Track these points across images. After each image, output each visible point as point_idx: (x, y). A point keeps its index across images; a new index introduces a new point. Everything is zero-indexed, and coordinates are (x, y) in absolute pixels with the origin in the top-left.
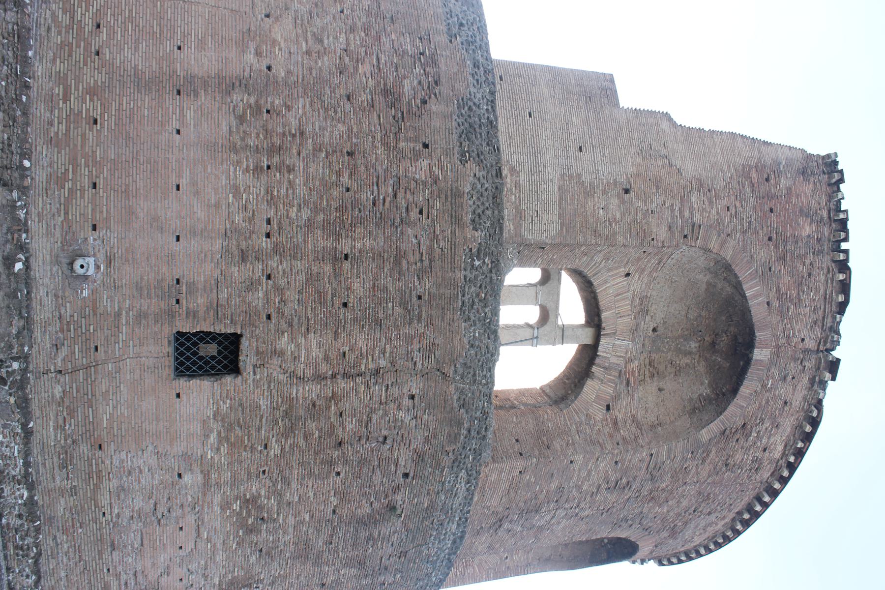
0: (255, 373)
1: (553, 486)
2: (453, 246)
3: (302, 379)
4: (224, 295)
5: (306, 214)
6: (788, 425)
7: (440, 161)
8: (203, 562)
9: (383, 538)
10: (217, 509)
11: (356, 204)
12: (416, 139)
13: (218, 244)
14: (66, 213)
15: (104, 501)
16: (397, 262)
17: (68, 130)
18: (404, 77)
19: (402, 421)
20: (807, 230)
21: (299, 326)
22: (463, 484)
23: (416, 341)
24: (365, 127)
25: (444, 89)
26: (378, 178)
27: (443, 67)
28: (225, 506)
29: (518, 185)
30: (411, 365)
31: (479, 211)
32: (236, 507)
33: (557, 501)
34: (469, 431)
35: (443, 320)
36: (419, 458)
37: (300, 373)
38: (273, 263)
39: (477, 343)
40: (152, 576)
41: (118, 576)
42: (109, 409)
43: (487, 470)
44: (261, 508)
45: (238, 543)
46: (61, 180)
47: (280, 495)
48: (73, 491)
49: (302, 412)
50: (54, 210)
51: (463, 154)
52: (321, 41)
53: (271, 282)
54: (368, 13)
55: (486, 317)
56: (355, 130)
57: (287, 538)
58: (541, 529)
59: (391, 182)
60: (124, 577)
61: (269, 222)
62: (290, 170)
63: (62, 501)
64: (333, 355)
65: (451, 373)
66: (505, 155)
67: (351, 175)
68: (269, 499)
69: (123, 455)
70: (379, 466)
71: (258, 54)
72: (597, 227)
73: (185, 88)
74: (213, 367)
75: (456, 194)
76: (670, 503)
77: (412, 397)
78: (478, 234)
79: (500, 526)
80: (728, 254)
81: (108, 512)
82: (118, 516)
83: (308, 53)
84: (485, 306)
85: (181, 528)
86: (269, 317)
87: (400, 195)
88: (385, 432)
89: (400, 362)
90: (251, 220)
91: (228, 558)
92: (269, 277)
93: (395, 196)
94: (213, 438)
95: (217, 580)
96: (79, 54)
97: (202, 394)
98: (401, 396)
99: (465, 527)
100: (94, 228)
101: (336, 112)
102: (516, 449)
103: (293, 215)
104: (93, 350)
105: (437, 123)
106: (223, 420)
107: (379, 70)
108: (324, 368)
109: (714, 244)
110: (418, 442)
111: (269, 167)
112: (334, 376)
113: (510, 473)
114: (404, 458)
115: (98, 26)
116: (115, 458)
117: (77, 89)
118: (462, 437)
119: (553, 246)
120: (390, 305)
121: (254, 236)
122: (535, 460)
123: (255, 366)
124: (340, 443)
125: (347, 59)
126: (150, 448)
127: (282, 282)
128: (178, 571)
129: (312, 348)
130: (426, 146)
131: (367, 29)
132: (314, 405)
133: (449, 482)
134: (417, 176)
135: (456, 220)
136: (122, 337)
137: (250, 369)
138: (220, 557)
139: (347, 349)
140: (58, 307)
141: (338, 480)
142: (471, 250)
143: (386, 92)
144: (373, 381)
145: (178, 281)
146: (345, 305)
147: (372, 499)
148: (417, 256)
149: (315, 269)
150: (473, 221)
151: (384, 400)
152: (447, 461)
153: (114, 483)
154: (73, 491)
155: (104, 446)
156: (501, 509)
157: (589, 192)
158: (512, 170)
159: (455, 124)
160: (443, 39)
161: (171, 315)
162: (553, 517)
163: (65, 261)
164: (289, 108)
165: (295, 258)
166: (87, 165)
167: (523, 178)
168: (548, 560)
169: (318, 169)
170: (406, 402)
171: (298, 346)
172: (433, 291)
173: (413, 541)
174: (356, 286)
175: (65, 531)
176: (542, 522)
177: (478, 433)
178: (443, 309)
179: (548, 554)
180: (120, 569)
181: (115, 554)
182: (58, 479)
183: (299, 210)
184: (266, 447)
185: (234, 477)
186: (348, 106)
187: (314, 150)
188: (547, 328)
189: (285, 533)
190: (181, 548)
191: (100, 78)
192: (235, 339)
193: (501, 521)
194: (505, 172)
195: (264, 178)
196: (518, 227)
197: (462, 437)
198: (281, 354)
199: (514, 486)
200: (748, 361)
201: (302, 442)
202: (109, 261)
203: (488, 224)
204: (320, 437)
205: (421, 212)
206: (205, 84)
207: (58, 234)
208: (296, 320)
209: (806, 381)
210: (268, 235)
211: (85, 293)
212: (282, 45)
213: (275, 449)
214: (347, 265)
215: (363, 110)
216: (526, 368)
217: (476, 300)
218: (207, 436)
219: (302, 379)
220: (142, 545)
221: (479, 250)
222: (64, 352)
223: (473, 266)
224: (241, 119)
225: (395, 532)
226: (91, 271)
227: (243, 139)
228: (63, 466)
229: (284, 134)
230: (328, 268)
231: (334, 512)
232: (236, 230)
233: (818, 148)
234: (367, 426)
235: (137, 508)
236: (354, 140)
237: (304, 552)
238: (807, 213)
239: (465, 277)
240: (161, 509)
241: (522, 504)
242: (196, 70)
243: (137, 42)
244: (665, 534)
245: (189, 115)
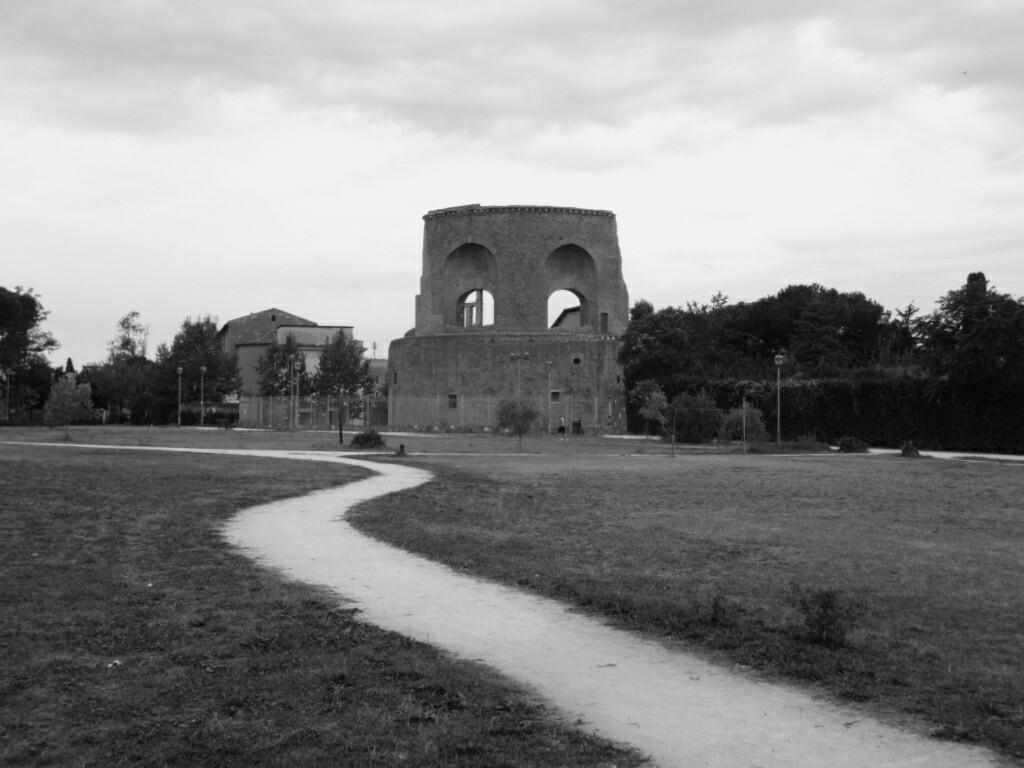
1: (508, 302)
6: (494, 217)
20: (439, 228)
76: (525, 251)
80: (445, 258)
97: (461, 402)
109: (443, 264)
129: (452, 380)
176: (526, 301)
200: (472, 244)
209: (478, 218)
233: (423, 223)
237: (503, 378)
238: (436, 227)
244: (549, 242)
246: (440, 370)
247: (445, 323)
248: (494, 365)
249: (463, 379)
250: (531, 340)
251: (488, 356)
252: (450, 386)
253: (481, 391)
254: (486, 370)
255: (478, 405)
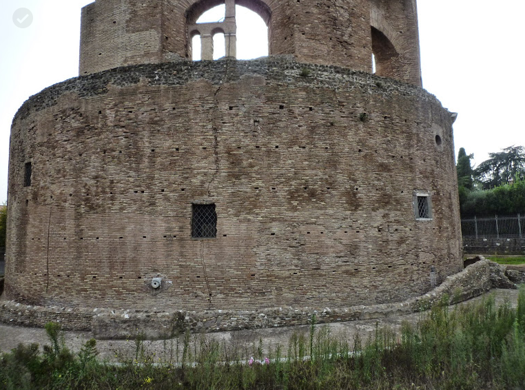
0: (213, 196)
1: (315, 11)
2: (147, 92)
3: (218, 170)
4: (171, 214)
5: (132, 173)
7: (106, 104)
8: (333, 220)
9: (327, 117)
10: (296, 214)
11: (127, 147)
12: (97, 118)
13: (147, 217)
14: (133, 291)
15: (287, 274)
16: (156, 123)
17: (98, 290)
18: (71, 127)
19: (245, 112)
21: (188, 173)
22: (293, 71)
23: (197, 109)
24: (92, 145)
25: (76, 104)
26: (115, 137)
27: (67, 106)
28: (294, 209)
29: (132, 57)
30: (211, 111)
31: (131, 79)
32: (295, 203)
33: (329, 7)
34: (255, 71)
35: (185, 94)
36: (269, 100)
37: (213, 171)
38: (156, 189)
39: (201, 73)
40: (341, 247)
41: (339, 266)
42: (232, 271)
43: (299, 56)
44: (297, 191)
45: (322, 201)
46: (119, 293)
47: (289, 179)
48: (279, 289)
49: (237, 170)
50: (131, 296)
51: (104, 92)
52: (60, 170)
53: (165, 190)
54: (48, 147)
55: (187, 69)
56: (94, 150)
57: (320, 174)
58: (352, 14)
59: (117, 129)
60: (340, 263)
61: (136, 192)
62: (112, 182)
63: (286, 294)
64: (205, 154)
65: (217, 86)
66: (118, 65)
67: (114, 151)
68: (291, 185)
69: (258, 264)
70: (274, 124)
71: (65, 201)
72: (152, 7)
73: (80, 235)
74: (212, 217)
75: (122, 93)
77: (231, 108)
78: (141, 79)
79: (346, 42)
81: (293, 272)
82: (296, 266)
83: (64, 176)
84: (181, 70)
85: (308, 233)
86: (183, 190)
87: (122, 124)
88: (252, 121)
89: (210, 117)
90: (135, 201)
91: (331, 207)
92: (163, 191)
93: (123, 127)
94: (249, 217)
95: (348, 213)
96: (69, 285)
97: (227, 224)
98: (230, 114)
99: (327, 66)
100: (140, 278)
101: (87, 161)
102: (289, 39)
103: (131, 180)
104: (199, 279)
105: (90, 107)
106: (240, 212)
107: (69, 140)
108: (212, 158)
110: (260, 102)
111: (111, 193)
112: (216, 153)
113: (303, 41)
114: (267, 109)
115: (59, 276)
116: (259, 266)
117: (82, 285)
118: (258, 76)
119: (163, 31)
120: (177, 125)
121: (143, 199)
122: (295, 26)
123: (209, 196)
124: (257, 147)
125: (66, 157)
126: (255, 250)
127: (166, 183)
128: (339, 233)
129: (203, 165)
130: (100, 112)
131: (54, 148)
132: (233, 163)
133: (290, 80)
134: (114, 116)
135: (134, 93)
136: (192, 264)
137: (211, 198)
138: (330, 211)
139: (201, 147)
140: (177, 295)
141: (280, 146)
142: (149, 82)
143: (78, 136)
144: (220, 131)
145: (165, 237)
146: (177, 149)
147: (297, 126)
148: (153, 112)
149: (159, 167)
150: (135, 82)
151: (231, 124)
152: (273, 83)
153: (275, 268)
154: (279, 289)
155: (253, 273)
156: (331, 44)
157: (134, 13)
158: (125, 61)
159: (91, 97)
160: (56, 107)
161: (182, 239)
162: (342, 7)
163: (154, 292)
164: (86, 185)
165: (153, 178)
166: (112, 281)
167: (129, 54)
168: (404, 4)
169: (112, 168)
170: (233, 111)
171: (198, 174)
172: (170, 101)
173: (331, 99)
174: (167, 144)
175: (305, 293)
176: (346, 15)
177: (257, 66)
178: (180, 95)
179: (400, 6)
180: (333, 265)
181: (322, 268)
182: (271, 297)
183: (130, 177)
184: (257, 188)
185: (275, 205)
186: (84, 155)
187: (103, 171)
188: (224, 28)
189: (316, 175)
190: (322, 233)
191: (78, 275)
192: (194, 206)
193: (341, 42)
194: (126, 65)
195: (117, 195)
196: (153, 54)
197: (258, 76)
198: (203, 182)
199: (313, 37)
201: (256, 168)
202: (155, 271)
203: (137, 73)
204: (252, 158)
205: (131, 112)
206: (78, 226)
207: (142, 295)
208: (185, 175)
210: (143, 192)
211: (170, 282)
212: (62, 189)
213: (260, 183)
214: (157, 150)
215: (85, 147)
216: (252, 38)
217: (178, 75)
218: (249, 220)
219: (218, 170)
220: (317, 253)
221: (150, 78)
222: (199, 293)
223: (159, 80)
224: (91, 208)
225: (322, 110)
226: (159, 279)
227: (100, 207)
228: (263, 294)
229: (97, 186)
230: (159, 160)
231: (304, 148)
232: (140, 209)
234: (247, 133)
235: (292, 256)
236: (99, 150)
237: (332, 163)
239: (164, 84)
240: (294, 243)
241: (328, 30)
242: (72, 231)
243: (63, 258)
245: (90, 233)
246: (167, 144)
247: (163, 49)
248: (313, 129)
249: (235, 161)
250: (378, 85)
251: (297, 111)
252: (196, 181)
253: (282, 192)
254: (292, 143)
255: (276, 228)
